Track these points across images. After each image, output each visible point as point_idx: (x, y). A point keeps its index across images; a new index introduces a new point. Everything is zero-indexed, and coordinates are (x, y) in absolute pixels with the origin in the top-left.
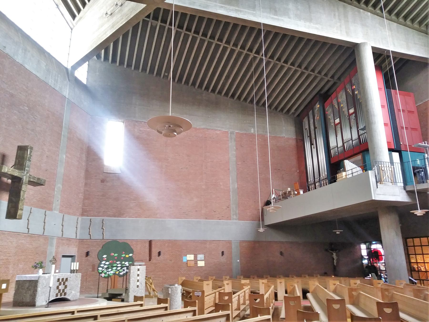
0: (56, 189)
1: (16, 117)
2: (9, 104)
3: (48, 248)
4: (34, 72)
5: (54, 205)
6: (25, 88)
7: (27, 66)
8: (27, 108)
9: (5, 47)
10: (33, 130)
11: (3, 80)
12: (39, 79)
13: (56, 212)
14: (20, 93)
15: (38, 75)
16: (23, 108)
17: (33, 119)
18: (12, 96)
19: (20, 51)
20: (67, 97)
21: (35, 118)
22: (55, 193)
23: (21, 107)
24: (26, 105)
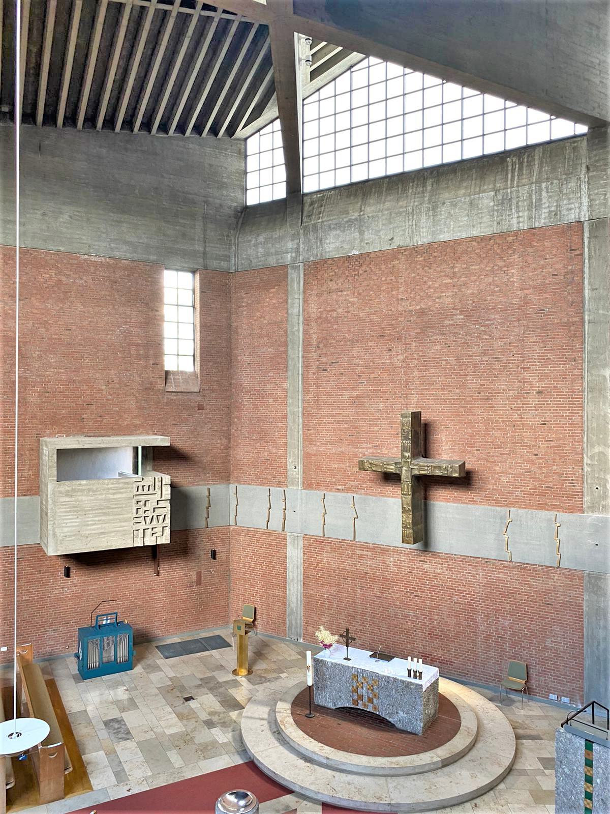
0: (586, 460)
1: (438, 347)
2: (419, 331)
3: (586, 597)
4: (464, 235)
5: (587, 498)
6: (448, 281)
7: (444, 237)
8: (462, 317)
9: (393, 238)
10: (484, 353)
11: (400, 297)
12: (482, 239)
13: (596, 515)
14: (439, 298)
15: (475, 232)
16: (451, 322)
17: (483, 328)
18: (422, 312)
19: (424, 218)
20: (585, 216)
21: (488, 326)
22: (586, 468)
23: (447, 322)
24: (455, 312)
